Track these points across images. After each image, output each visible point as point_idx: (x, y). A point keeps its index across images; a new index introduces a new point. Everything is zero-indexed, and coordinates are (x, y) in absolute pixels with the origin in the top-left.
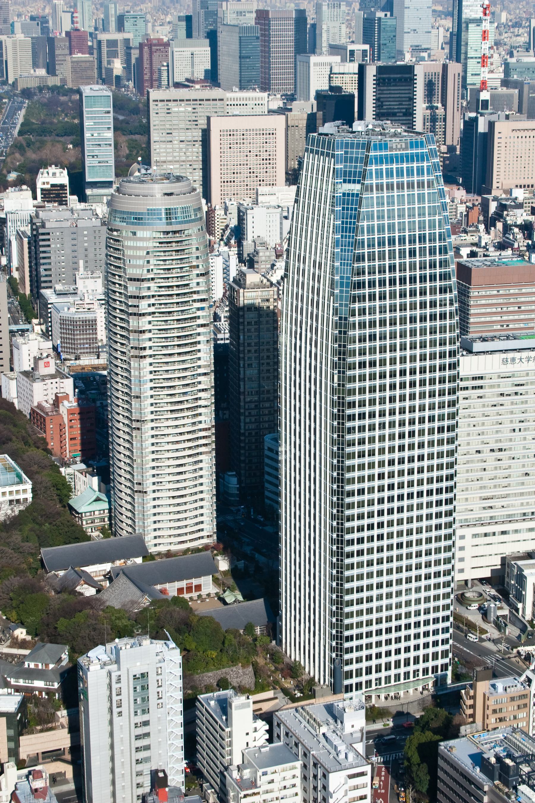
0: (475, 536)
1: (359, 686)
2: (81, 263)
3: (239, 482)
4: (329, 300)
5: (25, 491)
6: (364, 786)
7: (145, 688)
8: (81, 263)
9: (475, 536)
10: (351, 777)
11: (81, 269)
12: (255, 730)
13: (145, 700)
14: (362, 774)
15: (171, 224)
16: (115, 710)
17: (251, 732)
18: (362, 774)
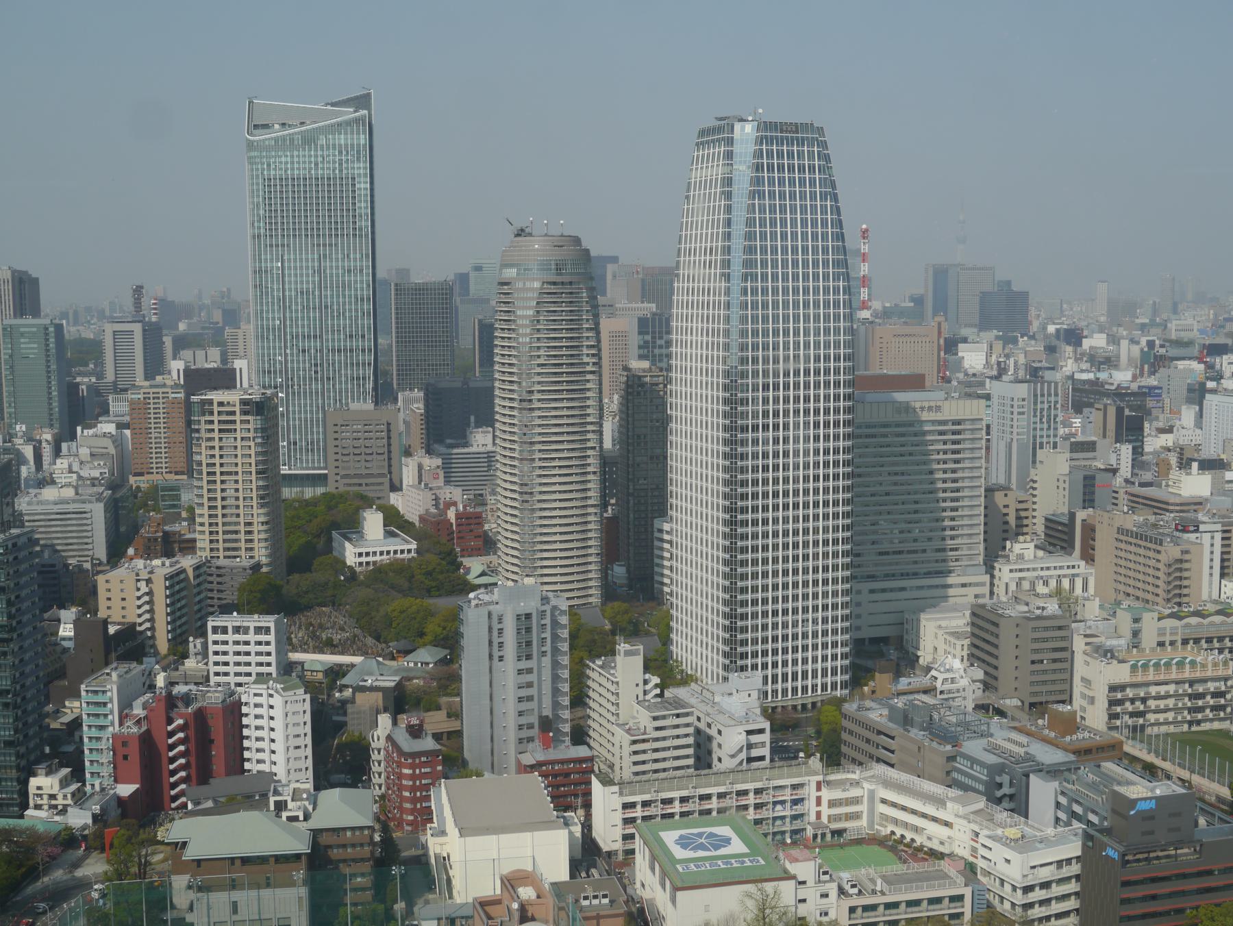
0: (872, 591)
1: (755, 667)
2: (472, 418)
3: (628, 571)
4: (720, 281)
5: (409, 551)
6: (763, 744)
7: (529, 630)
8: (472, 418)
9: (872, 591)
10: (749, 733)
11: (473, 425)
12: (646, 682)
13: (529, 644)
14: (761, 731)
15: (561, 274)
16: (496, 654)
17: (641, 683)
18: (761, 731)
